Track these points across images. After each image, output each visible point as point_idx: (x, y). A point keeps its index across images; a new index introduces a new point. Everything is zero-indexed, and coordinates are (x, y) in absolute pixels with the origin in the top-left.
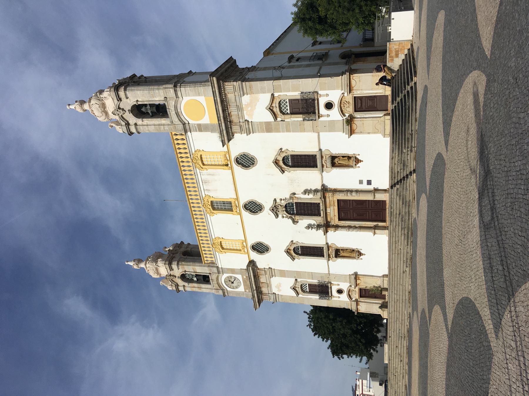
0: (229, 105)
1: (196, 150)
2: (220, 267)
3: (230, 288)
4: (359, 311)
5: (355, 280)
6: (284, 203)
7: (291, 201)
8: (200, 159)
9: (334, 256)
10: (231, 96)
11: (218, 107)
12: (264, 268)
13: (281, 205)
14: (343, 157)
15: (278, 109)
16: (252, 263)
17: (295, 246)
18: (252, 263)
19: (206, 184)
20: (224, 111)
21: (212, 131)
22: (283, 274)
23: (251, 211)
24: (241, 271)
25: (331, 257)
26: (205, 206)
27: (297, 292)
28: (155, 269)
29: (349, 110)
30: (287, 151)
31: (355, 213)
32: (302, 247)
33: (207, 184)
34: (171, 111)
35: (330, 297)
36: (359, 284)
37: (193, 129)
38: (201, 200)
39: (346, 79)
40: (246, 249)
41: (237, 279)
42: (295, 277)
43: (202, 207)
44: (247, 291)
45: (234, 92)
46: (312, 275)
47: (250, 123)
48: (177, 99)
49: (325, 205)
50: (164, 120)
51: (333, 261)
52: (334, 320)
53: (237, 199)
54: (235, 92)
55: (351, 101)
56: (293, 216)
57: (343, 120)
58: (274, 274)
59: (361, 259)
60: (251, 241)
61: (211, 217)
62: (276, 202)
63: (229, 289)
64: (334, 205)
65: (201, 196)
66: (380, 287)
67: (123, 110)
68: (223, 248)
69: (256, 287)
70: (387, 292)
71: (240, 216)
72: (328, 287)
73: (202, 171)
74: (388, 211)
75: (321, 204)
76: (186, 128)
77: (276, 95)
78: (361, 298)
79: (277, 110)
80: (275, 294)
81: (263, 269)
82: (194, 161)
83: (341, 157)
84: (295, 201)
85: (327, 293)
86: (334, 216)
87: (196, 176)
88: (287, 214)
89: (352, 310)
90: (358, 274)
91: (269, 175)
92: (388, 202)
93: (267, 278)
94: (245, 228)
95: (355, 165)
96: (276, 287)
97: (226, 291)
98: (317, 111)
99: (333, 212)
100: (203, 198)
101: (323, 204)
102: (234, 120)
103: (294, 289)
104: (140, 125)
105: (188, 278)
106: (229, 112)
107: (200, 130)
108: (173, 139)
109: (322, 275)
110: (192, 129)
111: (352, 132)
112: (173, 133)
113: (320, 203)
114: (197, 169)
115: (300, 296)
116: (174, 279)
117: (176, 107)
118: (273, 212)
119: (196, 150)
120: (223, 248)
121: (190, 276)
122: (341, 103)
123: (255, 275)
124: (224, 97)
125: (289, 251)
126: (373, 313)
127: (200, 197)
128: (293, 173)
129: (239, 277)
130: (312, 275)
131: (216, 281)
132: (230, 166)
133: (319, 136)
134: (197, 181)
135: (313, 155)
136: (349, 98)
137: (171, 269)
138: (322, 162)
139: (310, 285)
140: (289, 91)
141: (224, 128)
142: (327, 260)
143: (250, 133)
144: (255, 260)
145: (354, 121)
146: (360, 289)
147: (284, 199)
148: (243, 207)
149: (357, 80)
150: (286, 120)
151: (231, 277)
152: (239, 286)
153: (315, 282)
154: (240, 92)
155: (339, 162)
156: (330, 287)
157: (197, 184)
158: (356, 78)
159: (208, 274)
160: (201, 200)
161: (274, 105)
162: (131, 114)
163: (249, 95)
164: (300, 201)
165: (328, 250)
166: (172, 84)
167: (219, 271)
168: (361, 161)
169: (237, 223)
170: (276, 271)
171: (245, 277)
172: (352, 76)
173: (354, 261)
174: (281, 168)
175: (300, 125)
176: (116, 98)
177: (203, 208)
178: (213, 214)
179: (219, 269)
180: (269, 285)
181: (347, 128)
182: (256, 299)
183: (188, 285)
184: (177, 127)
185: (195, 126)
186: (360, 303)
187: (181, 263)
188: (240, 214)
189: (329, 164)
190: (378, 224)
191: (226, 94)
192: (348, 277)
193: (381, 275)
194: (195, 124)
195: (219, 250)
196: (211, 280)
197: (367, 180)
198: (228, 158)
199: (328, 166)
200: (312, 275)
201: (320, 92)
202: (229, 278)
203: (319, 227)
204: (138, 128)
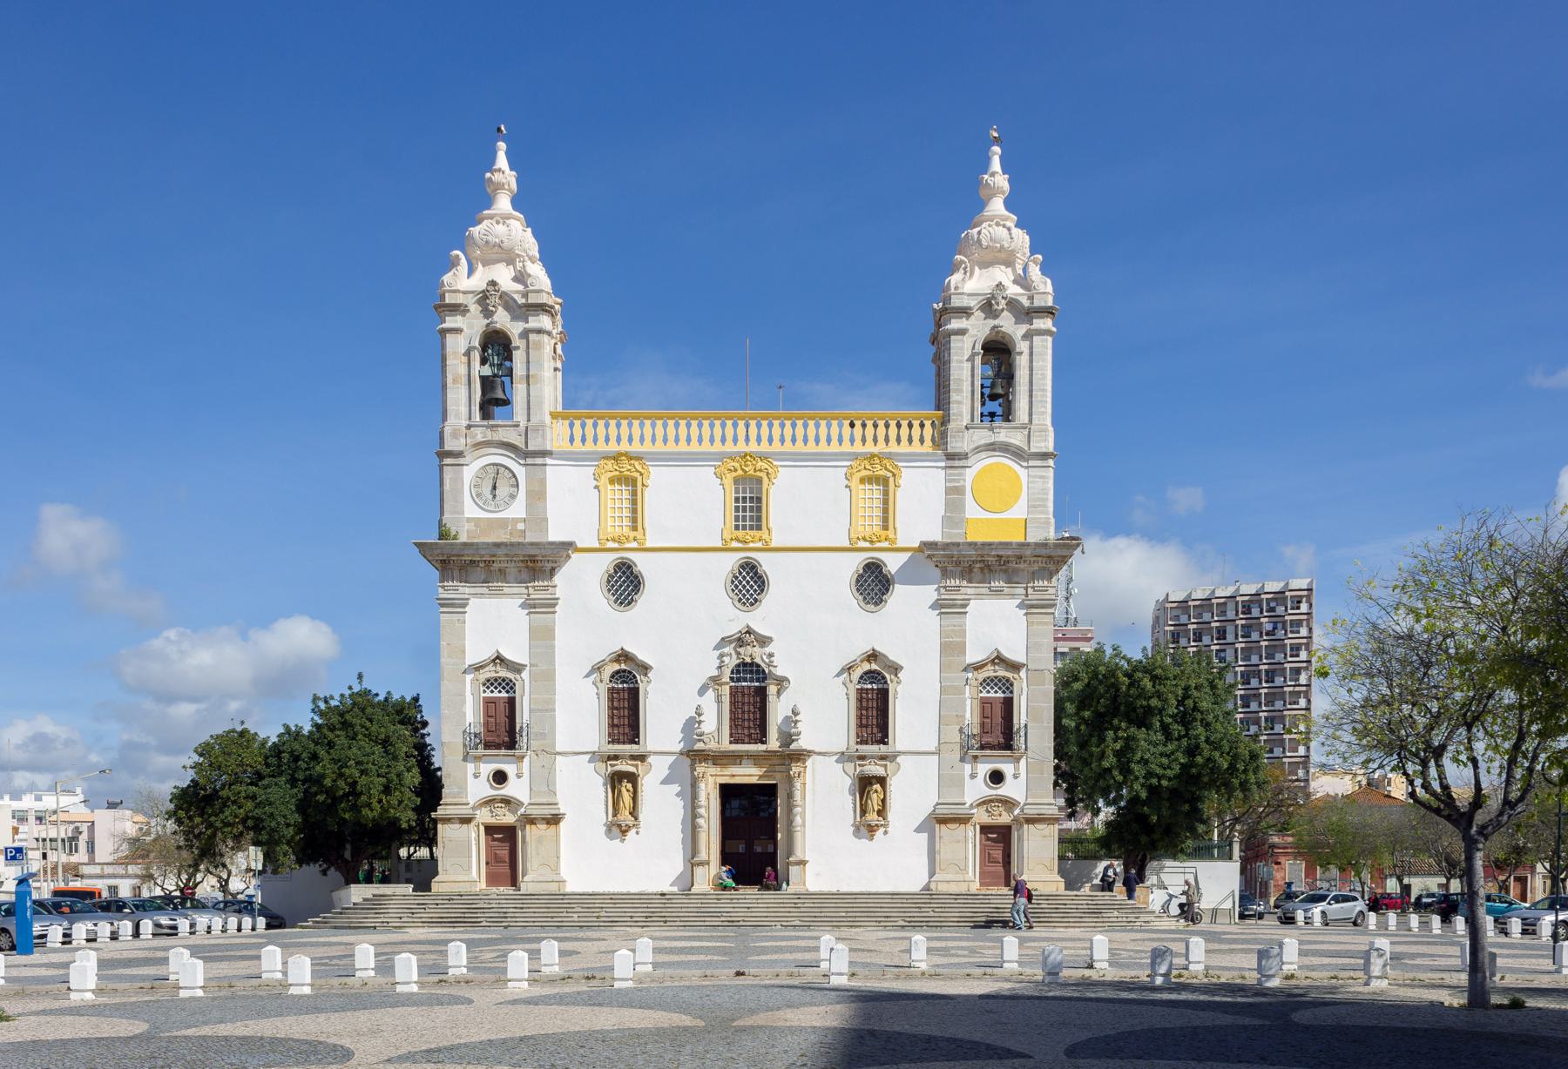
14: (884, 801)
22: (542, 638)
24: (537, 516)
37: (954, 475)
44: (471, 526)
46: (546, 709)
53: (768, 549)
57: (965, 804)
60: (642, 562)
75: (761, 747)
83: (882, 797)
84: (772, 689)
99: (748, 774)
103: (494, 661)
107: (948, 491)
110: (950, 471)
129: (517, 510)
130: (547, 710)
138: (872, 757)
150: (967, 687)
153: (524, 716)
165: (633, 757)
166: (1055, 448)
171: (521, 526)
194: (964, 480)
200: (547, 710)
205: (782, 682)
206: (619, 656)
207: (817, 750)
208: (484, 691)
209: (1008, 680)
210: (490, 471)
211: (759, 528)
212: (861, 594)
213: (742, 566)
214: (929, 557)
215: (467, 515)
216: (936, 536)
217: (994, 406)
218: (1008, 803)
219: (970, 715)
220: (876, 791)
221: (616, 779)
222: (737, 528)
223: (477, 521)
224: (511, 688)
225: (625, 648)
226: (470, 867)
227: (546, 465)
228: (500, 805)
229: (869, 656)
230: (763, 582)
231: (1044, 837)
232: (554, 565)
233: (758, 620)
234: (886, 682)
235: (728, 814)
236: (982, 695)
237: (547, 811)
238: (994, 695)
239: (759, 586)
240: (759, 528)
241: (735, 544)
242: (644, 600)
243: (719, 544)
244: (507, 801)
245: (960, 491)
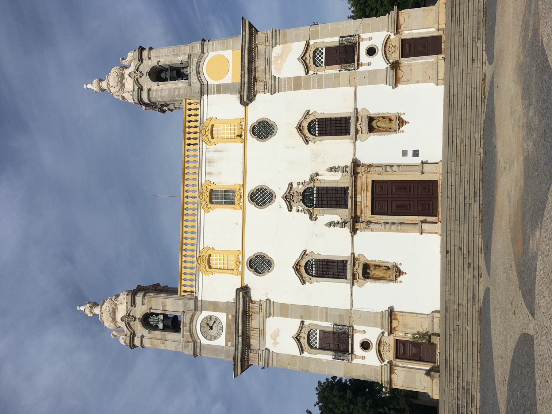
0: (257, 59)
1: (208, 118)
2: (200, 299)
3: (206, 338)
4: (394, 387)
5: (390, 319)
6: (301, 188)
7: (311, 185)
8: (210, 130)
9: (361, 275)
10: (261, 48)
11: (245, 54)
12: (260, 300)
13: (297, 192)
14: (384, 118)
15: (311, 60)
16: (244, 291)
17: (308, 258)
18: (244, 291)
19: (210, 165)
20: (250, 62)
21: (232, 93)
23: (258, 204)
25: (356, 279)
26: (201, 197)
27: (302, 347)
28: (111, 310)
29: (395, 56)
30: (314, 114)
31: (394, 204)
32: (318, 261)
33: (211, 164)
34: (191, 70)
35: (350, 354)
36: (395, 328)
38: (198, 187)
39: (393, 16)
40: (241, 266)
41: (219, 321)
42: (301, 318)
43: (198, 197)
44: (229, 344)
45: (266, 42)
46: (326, 313)
47: (277, 80)
48: (202, 54)
49: (355, 187)
50: (182, 83)
51: (358, 286)
52: (352, 401)
53: (244, 185)
54: (267, 41)
55: (398, 44)
56: (311, 210)
57: (387, 68)
58: (272, 312)
59: (401, 282)
60: (249, 254)
61: (206, 214)
62: (291, 188)
63: (204, 341)
64: (367, 190)
65: (200, 182)
66: (427, 333)
67: (141, 72)
68: (210, 267)
69: (243, 333)
70: (439, 338)
71: (242, 211)
72: (348, 335)
73: (210, 147)
74: (440, 196)
75: (350, 188)
76: (203, 90)
77: (312, 42)
78: (397, 360)
79: (310, 61)
80: (269, 350)
81: (258, 301)
82: (202, 132)
84: (317, 184)
85: (346, 351)
86: (366, 206)
87: (201, 153)
88: (304, 206)
89: (382, 384)
90: (395, 310)
91: (288, 147)
92: (440, 182)
93: (262, 319)
94: (246, 237)
95: (399, 128)
96: (271, 336)
97: (198, 344)
98: (356, 57)
100: (201, 184)
101: (352, 187)
102: (259, 77)
103: (298, 340)
104: (154, 90)
105: (152, 323)
106: (256, 66)
107: (219, 92)
108: (186, 108)
109: (341, 314)
110: (210, 91)
111: (397, 81)
112: (188, 101)
113: (348, 187)
114: (204, 143)
115: (306, 354)
116: (131, 323)
117: (198, 65)
118: (285, 201)
119: (208, 118)
120: (210, 267)
121: (155, 321)
122: (385, 47)
123: (245, 310)
124: (253, 46)
125: (298, 267)
126: (415, 390)
127: (198, 182)
128: (319, 144)
129: (222, 317)
130: (327, 313)
131: (188, 325)
132: (243, 137)
133: (356, 90)
134: (199, 160)
135: (346, 118)
136: (395, 40)
137: (133, 304)
138: (356, 126)
140: (327, 37)
141: (246, 80)
142: (350, 285)
143: (274, 93)
144: (250, 286)
145: (400, 67)
146: (397, 340)
147: (303, 183)
148: (248, 197)
149: (406, 16)
150: (319, 73)
151: (211, 317)
152: (219, 334)
153: (328, 325)
154: (272, 40)
155: (378, 124)
156: (351, 333)
157: (199, 164)
158: (404, 14)
159: (180, 314)
160: (198, 187)
161: (307, 55)
162: (148, 77)
163: (281, 45)
164: (323, 185)
165: (354, 266)
166: (200, 41)
167: (198, 306)
168: (406, 122)
169: (237, 223)
170: (275, 306)
171: (230, 317)
172: (400, 12)
173: (391, 284)
174: (305, 137)
175: (334, 78)
176: (137, 58)
177: (199, 199)
178: (209, 209)
179: (197, 301)
180: (262, 333)
181: (391, 73)
182: (240, 355)
183: (149, 333)
184: (194, 89)
185: (214, 86)
186: (396, 368)
187: (148, 295)
188: (243, 208)
189: (364, 126)
190: (426, 219)
191: (256, 45)
192: (379, 316)
193: (429, 312)
194: (214, 85)
195: (204, 269)
196: (182, 324)
197: (413, 150)
198: (243, 128)
199: (363, 132)
200: (327, 313)
201: (363, 36)
202: (207, 320)
203: (344, 224)
204: (150, 93)
206: (297, 269)
209: (315, 52)
210: (204, 330)
212: (268, 136)
213: (253, 201)
215: (223, 344)
219: (333, 70)
221: (366, 275)
222: (233, 203)
223: (227, 340)
225: (293, 266)
227: (202, 300)
228: (382, 348)
229: (300, 130)
231: (409, 17)
235: (390, 212)
238: (324, 59)
240: (234, 192)
242: (270, 254)
243: (241, 211)
244: (380, 343)
245: (219, 86)
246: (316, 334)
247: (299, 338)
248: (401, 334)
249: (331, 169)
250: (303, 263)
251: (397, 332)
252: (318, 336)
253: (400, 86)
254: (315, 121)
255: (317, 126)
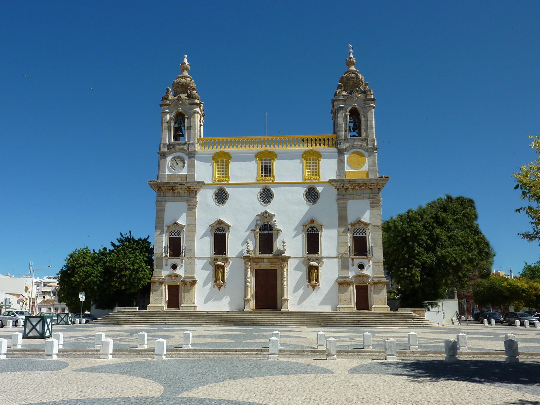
14: (318, 276)
42: (188, 225)
46: (192, 242)
57: (349, 277)
79: (358, 226)
99: (265, 266)
103: (174, 224)
105: (178, 119)
109: (192, 250)
139: (179, 239)
148: (266, 186)
153: (184, 244)
161: (362, 224)
205: (279, 231)
207: (292, 256)
208: (170, 235)
211: (270, 176)
214: (333, 185)
216: (334, 177)
217: (355, 133)
218: (366, 276)
219: (350, 243)
220: (315, 272)
222: (262, 176)
224: (180, 234)
225: (221, 219)
226: (162, 301)
230: (272, 195)
232: (196, 190)
233: (270, 209)
234: (317, 231)
236: (354, 235)
237: (190, 280)
239: (270, 196)
241: (261, 182)
242: (228, 202)
244: (176, 276)
246: (178, 235)
247: (175, 224)
248: (183, 288)
249: (284, 243)
250: (223, 226)
251: (184, 286)
252: (177, 236)
253: (337, 284)
254: (317, 231)
255: (314, 232)
